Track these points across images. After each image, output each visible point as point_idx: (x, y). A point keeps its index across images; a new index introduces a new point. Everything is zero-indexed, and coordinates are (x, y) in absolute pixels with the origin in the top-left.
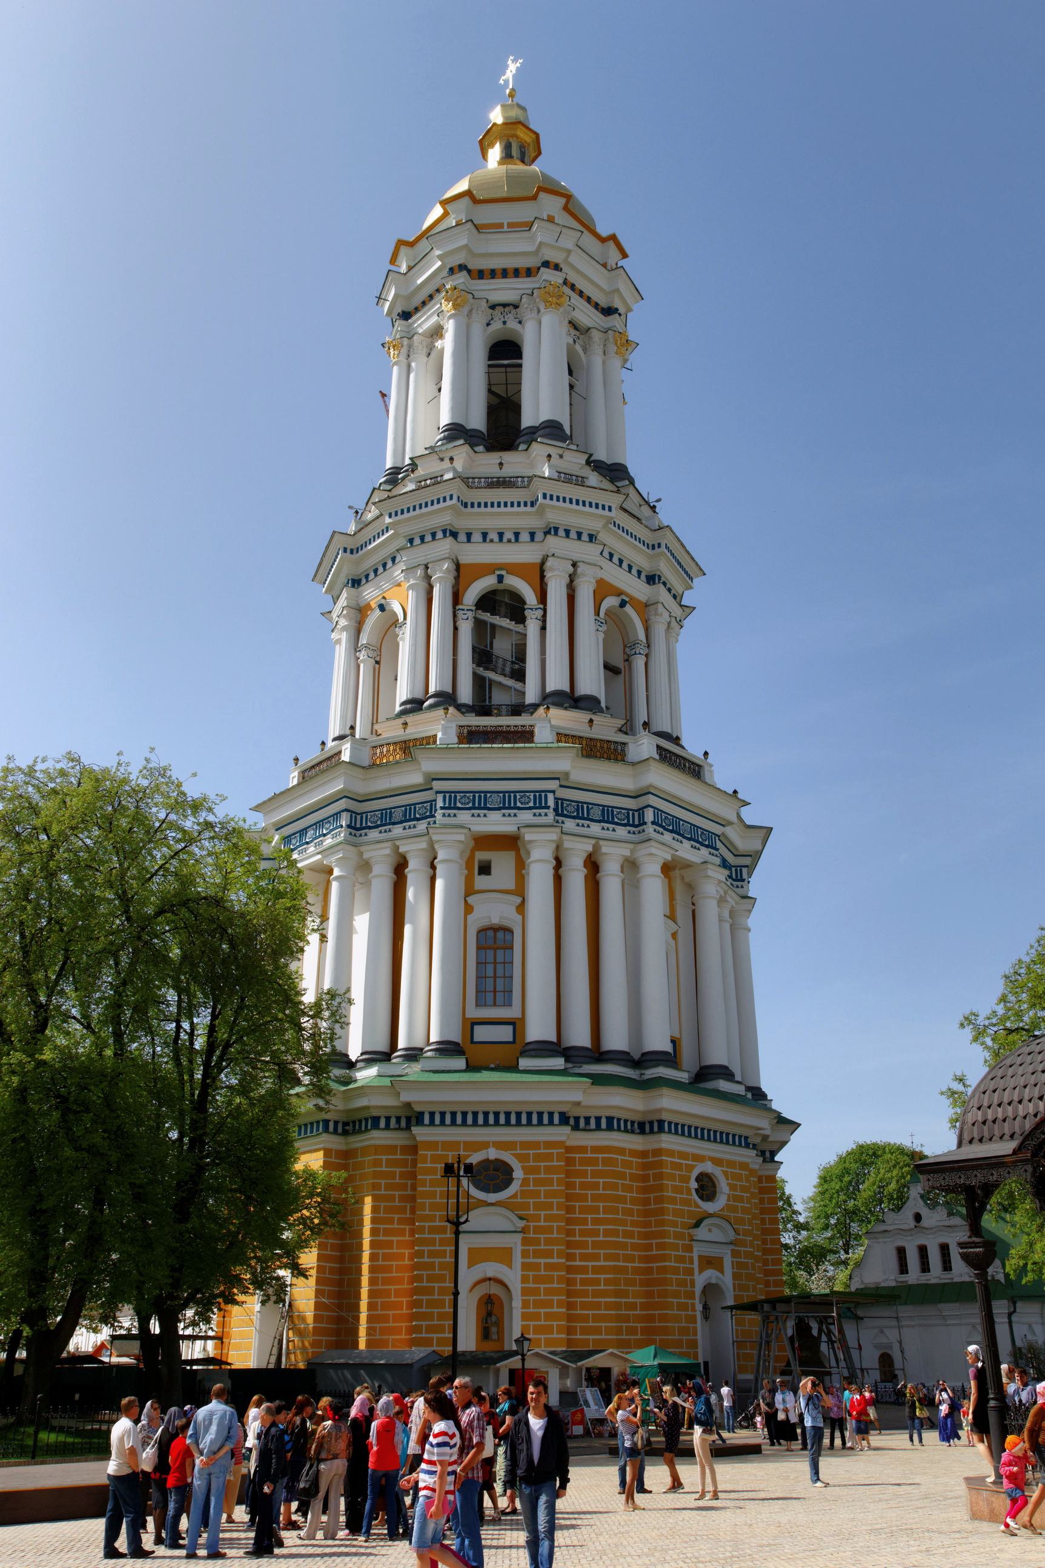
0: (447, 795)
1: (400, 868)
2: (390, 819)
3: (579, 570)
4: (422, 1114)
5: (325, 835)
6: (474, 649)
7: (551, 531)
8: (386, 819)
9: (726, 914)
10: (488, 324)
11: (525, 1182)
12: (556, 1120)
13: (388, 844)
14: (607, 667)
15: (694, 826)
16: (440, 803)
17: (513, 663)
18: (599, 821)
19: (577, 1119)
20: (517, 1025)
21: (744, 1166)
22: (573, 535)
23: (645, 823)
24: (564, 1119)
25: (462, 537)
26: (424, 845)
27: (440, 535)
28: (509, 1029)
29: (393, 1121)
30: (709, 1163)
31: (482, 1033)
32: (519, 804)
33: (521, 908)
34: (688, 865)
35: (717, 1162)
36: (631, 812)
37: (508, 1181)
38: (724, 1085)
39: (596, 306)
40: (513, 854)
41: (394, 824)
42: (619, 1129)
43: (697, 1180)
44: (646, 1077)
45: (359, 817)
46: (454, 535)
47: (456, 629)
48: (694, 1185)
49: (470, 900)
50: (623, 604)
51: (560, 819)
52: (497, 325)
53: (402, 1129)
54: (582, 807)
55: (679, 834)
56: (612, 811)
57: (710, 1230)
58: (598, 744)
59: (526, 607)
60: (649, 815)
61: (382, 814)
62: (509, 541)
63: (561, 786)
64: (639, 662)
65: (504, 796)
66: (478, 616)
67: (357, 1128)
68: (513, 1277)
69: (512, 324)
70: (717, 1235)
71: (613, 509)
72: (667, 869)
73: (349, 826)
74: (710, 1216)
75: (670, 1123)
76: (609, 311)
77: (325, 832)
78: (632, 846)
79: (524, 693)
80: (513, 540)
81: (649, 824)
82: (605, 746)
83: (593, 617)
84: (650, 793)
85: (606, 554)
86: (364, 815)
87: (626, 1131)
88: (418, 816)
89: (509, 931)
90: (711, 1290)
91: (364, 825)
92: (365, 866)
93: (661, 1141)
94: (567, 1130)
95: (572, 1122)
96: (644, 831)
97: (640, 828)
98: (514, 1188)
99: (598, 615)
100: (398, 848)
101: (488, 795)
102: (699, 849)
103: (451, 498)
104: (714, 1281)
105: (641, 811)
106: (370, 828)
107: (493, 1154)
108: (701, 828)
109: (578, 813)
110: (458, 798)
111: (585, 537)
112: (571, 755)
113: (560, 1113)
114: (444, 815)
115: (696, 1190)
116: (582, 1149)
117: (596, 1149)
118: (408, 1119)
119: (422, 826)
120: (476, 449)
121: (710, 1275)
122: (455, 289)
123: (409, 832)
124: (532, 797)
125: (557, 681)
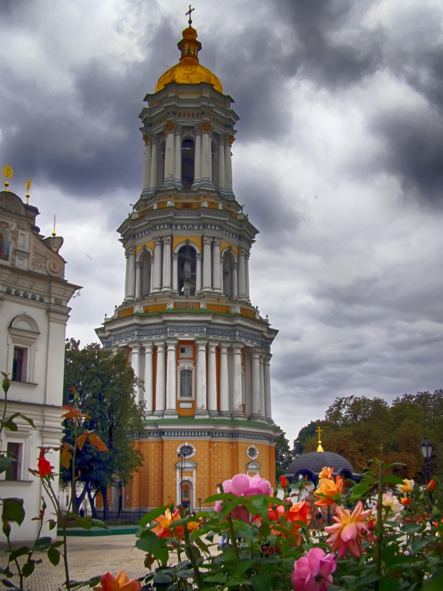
1: (155, 349)
3: (215, 240)
4: (165, 432)
5: (128, 337)
7: (205, 226)
9: (262, 361)
10: (182, 134)
11: (196, 452)
12: (206, 434)
13: (151, 342)
14: (224, 272)
16: (168, 330)
19: (212, 433)
20: (194, 403)
22: (213, 228)
24: (209, 434)
25: (174, 227)
27: (166, 227)
31: (182, 405)
32: (195, 331)
33: (195, 364)
34: (249, 347)
37: (191, 453)
41: (152, 335)
42: (225, 437)
43: (249, 450)
48: (248, 452)
49: (178, 362)
51: (208, 335)
52: (185, 135)
55: (247, 338)
57: (252, 465)
60: (237, 333)
64: (235, 272)
68: (193, 480)
70: (254, 467)
71: (227, 217)
72: (242, 350)
73: (137, 335)
74: (252, 461)
77: (128, 336)
85: (224, 232)
87: (227, 437)
94: (209, 437)
95: (211, 434)
97: (234, 337)
98: (193, 454)
100: (154, 344)
103: (170, 214)
105: (235, 331)
106: (144, 336)
107: (187, 444)
115: (249, 454)
116: (214, 442)
117: (218, 442)
118: (160, 433)
119: (162, 337)
122: (170, 122)
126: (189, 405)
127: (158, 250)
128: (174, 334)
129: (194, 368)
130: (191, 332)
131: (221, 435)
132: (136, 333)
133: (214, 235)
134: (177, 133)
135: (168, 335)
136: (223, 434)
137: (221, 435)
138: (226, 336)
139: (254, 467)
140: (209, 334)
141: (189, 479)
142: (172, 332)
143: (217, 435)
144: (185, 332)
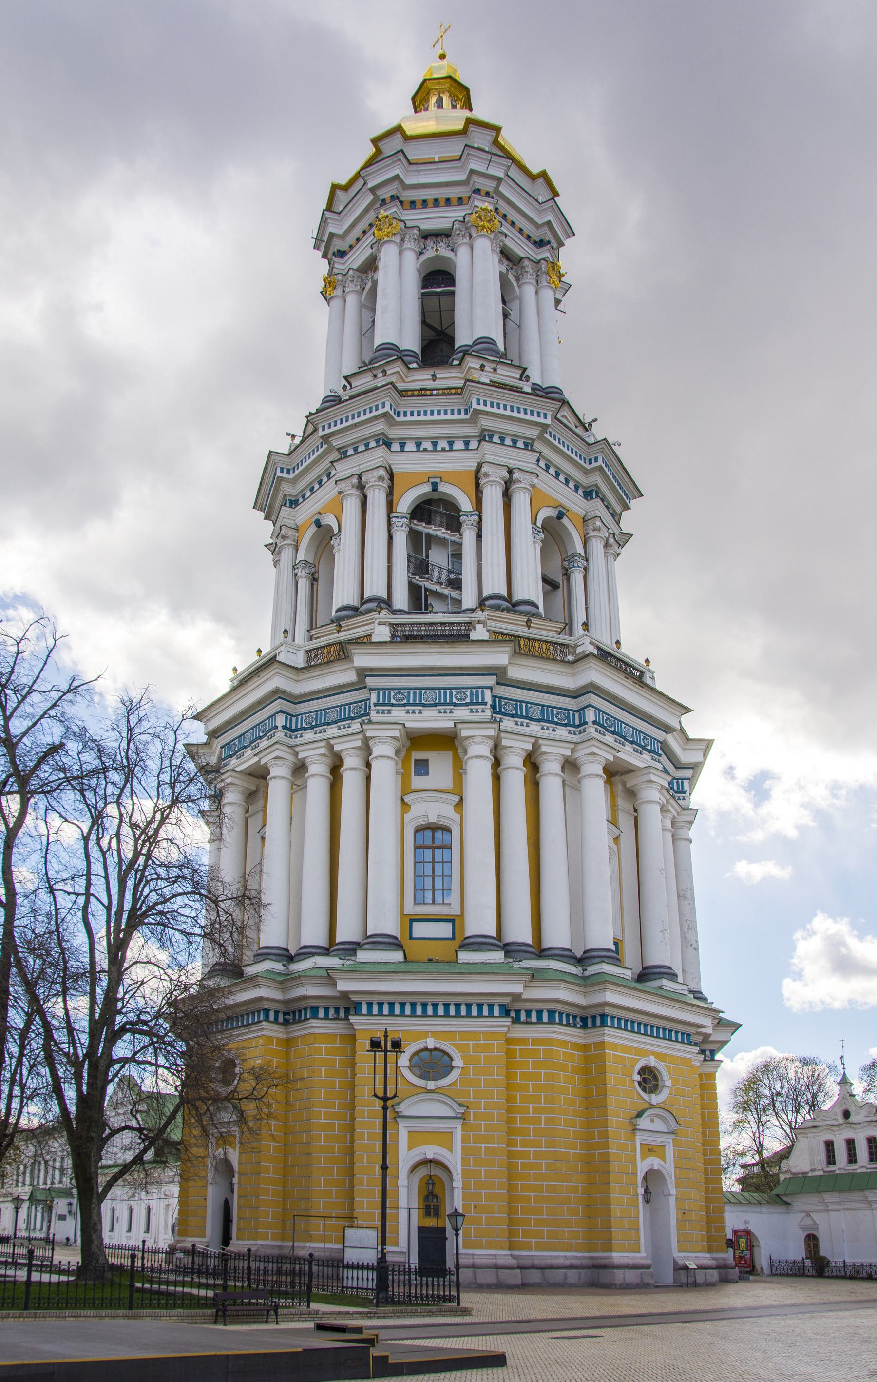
0: (381, 692)
2: (325, 720)
3: (517, 475)
4: (360, 1003)
6: (409, 556)
8: (321, 721)
10: (421, 253)
13: (323, 743)
15: (637, 730)
16: (374, 699)
17: (449, 572)
18: (539, 721)
19: (518, 1012)
21: (686, 1062)
23: (586, 723)
24: (506, 1011)
25: (396, 447)
26: (358, 743)
27: (373, 444)
28: (449, 925)
29: (332, 1013)
30: (652, 1058)
31: (421, 930)
32: (455, 700)
33: (459, 805)
34: (630, 770)
35: (660, 1056)
36: (571, 713)
37: (449, 1069)
38: (666, 983)
39: (529, 238)
40: (451, 753)
41: (329, 724)
42: (561, 1023)
43: (639, 1073)
44: (587, 973)
45: (294, 719)
46: (388, 444)
47: (390, 538)
48: (638, 1078)
49: (407, 799)
50: (560, 516)
52: (430, 254)
53: (341, 1019)
54: (521, 706)
55: (621, 736)
56: (552, 711)
57: (652, 1121)
58: (537, 645)
59: (461, 514)
60: (590, 716)
61: (317, 715)
62: (443, 450)
63: (498, 683)
65: (440, 693)
66: (412, 525)
67: (297, 1017)
68: (454, 1160)
69: (444, 252)
74: (652, 1106)
75: (613, 1018)
76: (540, 244)
78: (572, 746)
79: (459, 602)
80: (447, 449)
81: (590, 724)
82: (544, 646)
83: (529, 525)
84: (590, 692)
86: (300, 717)
88: (352, 715)
89: (448, 830)
90: (652, 1177)
91: (299, 726)
92: (300, 769)
93: (604, 1034)
95: (513, 1014)
96: (585, 731)
98: (454, 1075)
99: (535, 524)
100: (332, 747)
101: (423, 691)
102: (641, 754)
104: (656, 1168)
106: (305, 729)
107: (431, 1043)
108: (643, 733)
109: (516, 712)
110: (393, 694)
111: (520, 444)
112: (508, 649)
113: (499, 1005)
114: (378, 713)
115: (639, 1082)
116: (523, 1041)
117: (537, 1042)
119: (356, 726)
120: (411, 366)
121: (654, 1162)
123: (344, 732)
124: (468, 693)
125: (495, 585)
126: (444, 930)
127: (351, 506)
128: (389, 713)
129: (457, 817)
130: (445, 704)
131: (545, 1018)
132: (280, 720)
133: (513, 464)
134: (407, 245)
135: (374, 716)
136: (551, 1013)
137: (545, 1018)
138: (557, 724)
139: (658, 1125)
140: (500, 713)
141: (441, 1155)
142: (383, 704)
143: (534, 1018)
144: (424, 705)
